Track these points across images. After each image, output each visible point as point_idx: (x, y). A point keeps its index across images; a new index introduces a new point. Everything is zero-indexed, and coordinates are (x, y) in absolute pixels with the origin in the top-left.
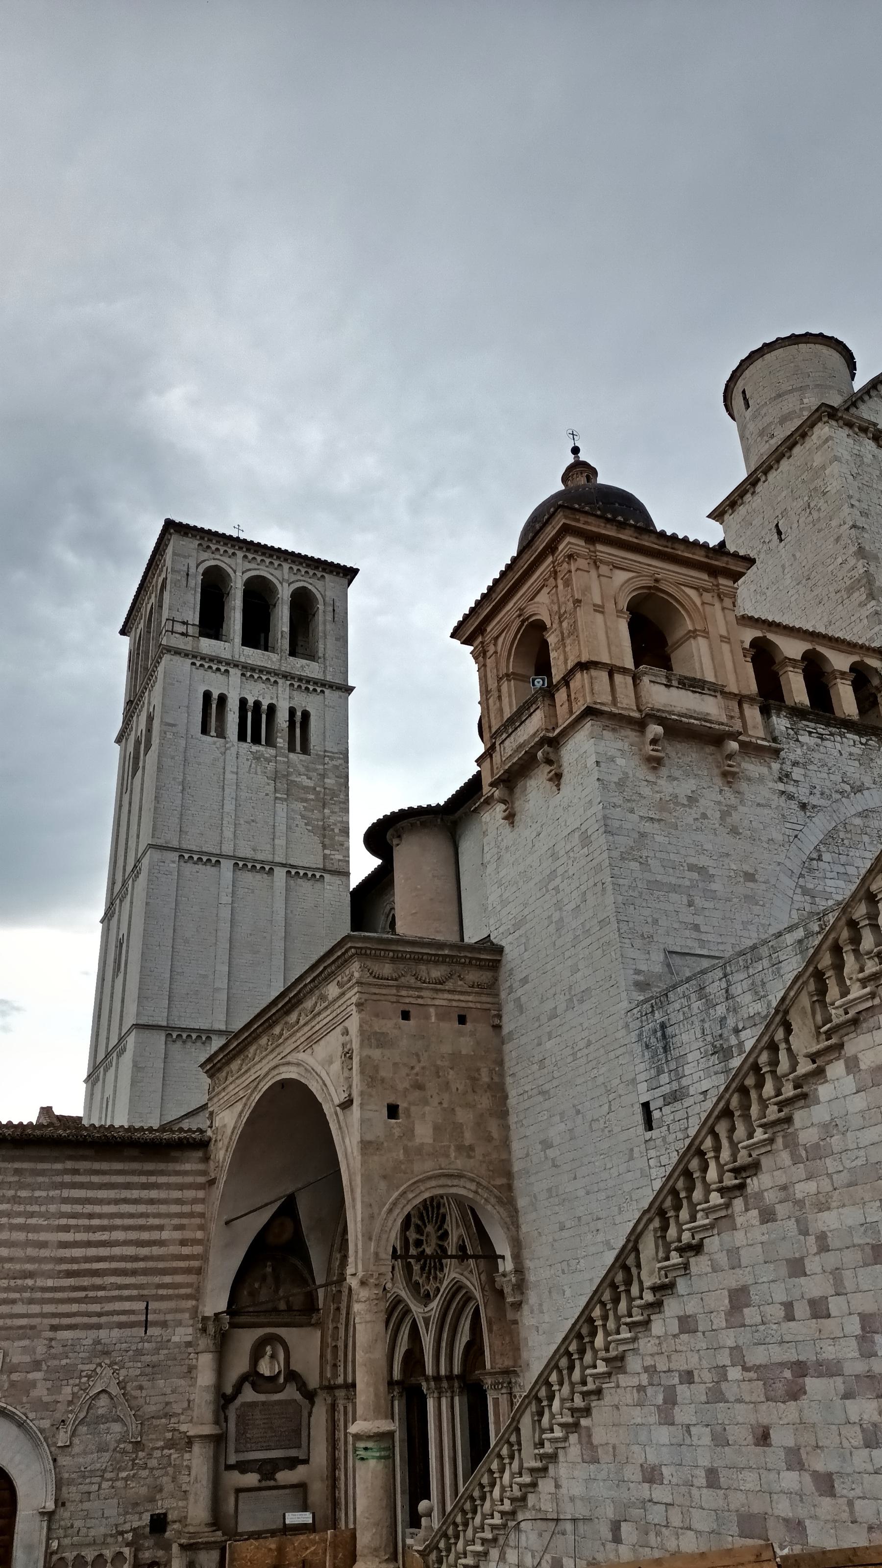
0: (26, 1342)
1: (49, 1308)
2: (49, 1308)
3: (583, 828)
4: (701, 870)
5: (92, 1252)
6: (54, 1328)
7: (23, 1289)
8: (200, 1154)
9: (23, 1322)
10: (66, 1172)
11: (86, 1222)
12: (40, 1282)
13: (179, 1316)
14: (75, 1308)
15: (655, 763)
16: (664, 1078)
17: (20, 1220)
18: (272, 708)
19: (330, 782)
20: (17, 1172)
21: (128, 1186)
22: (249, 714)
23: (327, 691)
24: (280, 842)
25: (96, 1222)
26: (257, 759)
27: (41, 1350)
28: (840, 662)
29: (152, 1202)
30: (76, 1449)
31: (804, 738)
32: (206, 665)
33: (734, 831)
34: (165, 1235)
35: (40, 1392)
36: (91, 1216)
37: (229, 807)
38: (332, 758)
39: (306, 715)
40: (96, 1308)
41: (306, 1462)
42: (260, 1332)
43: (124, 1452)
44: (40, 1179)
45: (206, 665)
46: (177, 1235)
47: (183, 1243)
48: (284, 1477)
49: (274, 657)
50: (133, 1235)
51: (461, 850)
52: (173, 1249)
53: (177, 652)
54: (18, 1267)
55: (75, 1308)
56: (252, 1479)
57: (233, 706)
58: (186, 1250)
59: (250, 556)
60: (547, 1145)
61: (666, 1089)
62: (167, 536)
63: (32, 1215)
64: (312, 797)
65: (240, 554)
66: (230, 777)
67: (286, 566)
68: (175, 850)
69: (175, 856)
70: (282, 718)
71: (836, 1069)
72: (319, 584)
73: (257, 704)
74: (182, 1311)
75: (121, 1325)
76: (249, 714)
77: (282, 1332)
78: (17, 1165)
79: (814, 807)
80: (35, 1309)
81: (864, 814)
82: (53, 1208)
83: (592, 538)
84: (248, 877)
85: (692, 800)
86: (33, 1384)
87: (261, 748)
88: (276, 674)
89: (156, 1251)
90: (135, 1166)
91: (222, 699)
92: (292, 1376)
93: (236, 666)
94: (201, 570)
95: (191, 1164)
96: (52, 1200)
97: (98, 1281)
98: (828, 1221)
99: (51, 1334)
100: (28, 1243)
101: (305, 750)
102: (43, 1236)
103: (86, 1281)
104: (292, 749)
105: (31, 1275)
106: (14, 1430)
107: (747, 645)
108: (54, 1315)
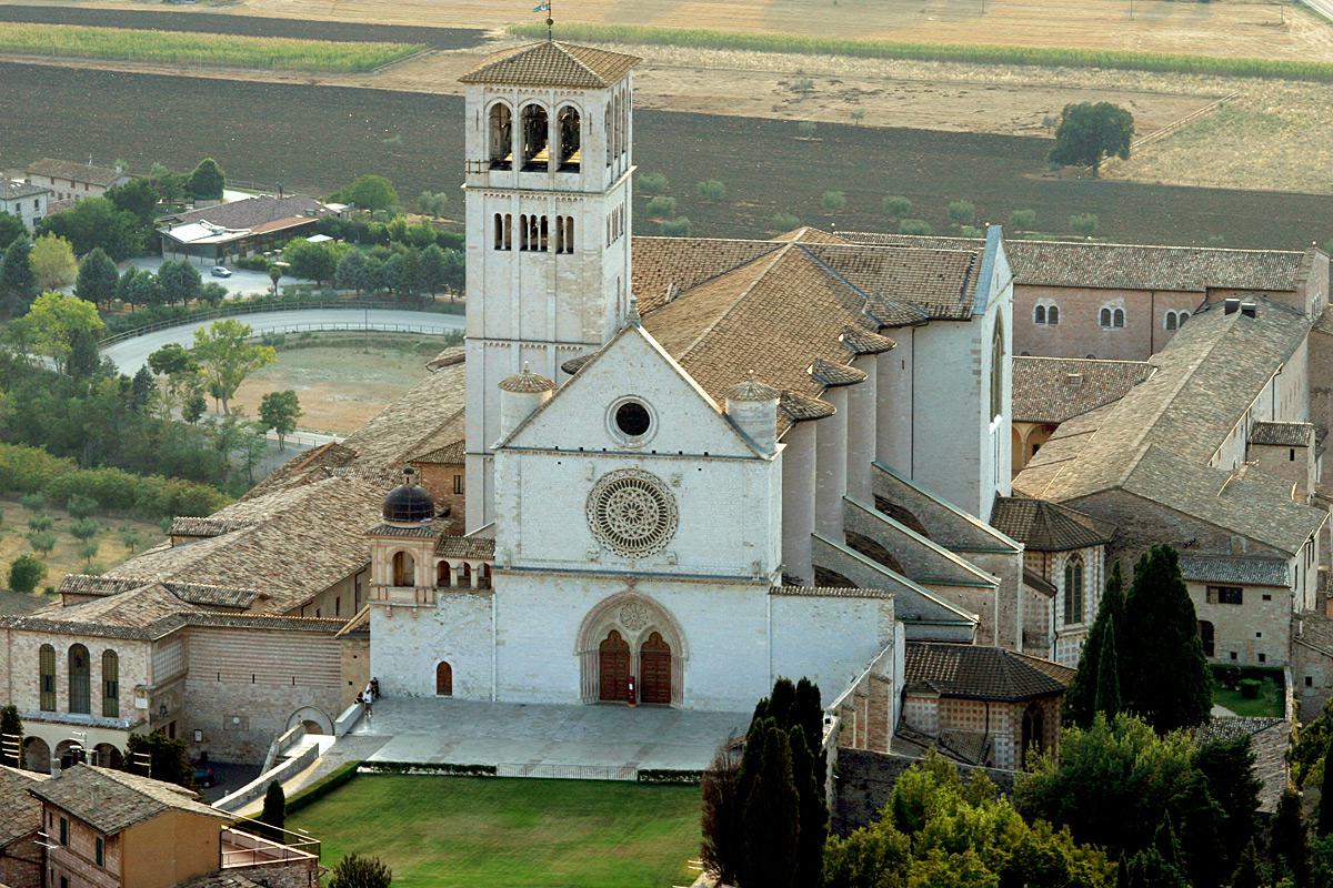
18: (544, 218)
23: (585, 199)
31: (449, 599)
33: (415, 634)
35: (326, 704)
37: (515, 304)
39: (570, 219)
57: (516, 223)
59: (523, 89)
65: (516, 89)
67: (552, 91)
70: (552, 226)
73: (533, 218)
79: (447, 624)
81: (468, 623)
85: (401, 626)
91: (508, 216)
94: (488, 110)
101: (570, 251)
104: (560, 251)
107: (436, 565)
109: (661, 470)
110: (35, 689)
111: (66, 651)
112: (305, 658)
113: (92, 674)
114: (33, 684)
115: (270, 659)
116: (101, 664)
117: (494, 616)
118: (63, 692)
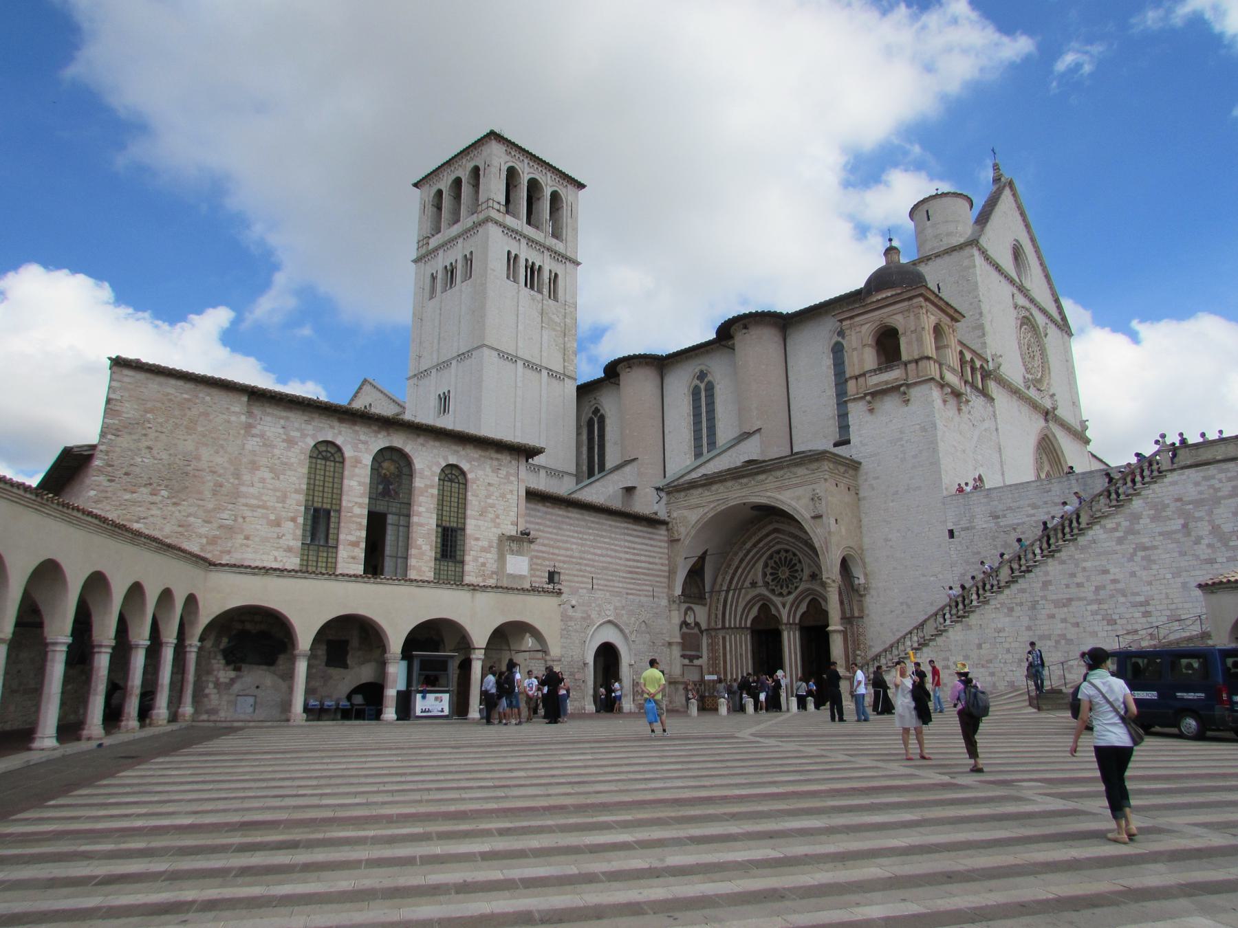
0: (618, 598)
1: (625, 585)
2: (625, 585)
3: (922, 425)
4: (955, 447)
5: (635, 564)
6: (627, 594)
7: (616, 576)
8: (664, 527)
9: (618, 590)
10: (625, 528)
11: (632, 551)
12: (621, 574)
13: (662, 595)
14: (632, 586)
15: (945, 401)
16: (962, 522)
17: (613, 547)
19: (568, 321)
20: (610, 526)
21: (644, 538)
22: (529, 270)
23: (568, 263)
24: (544, 354)
25: (636, 551)
26: (533, 300)
27: (624, 601)
28: (978, 364)
29: (651, 546)
30: (637, 643)
32: (510, 234)
34: (657, 560)
36: (634, 549)
38: (569, 307)
39: (556, 275)
40: (638, 588)
41: (701, 657)
42: (687, 605)
43: (650, 646)
44: (617, 530)
45: (510, 234)
46: (661, 561)
47: (662, 565)
48: (696, 662)
49: (542, 235)
50: (647, 559)
51: (665, 381)
52: (659, 567)
53: (496, 222)
54: (614, 567)
55: (632, 586)
56: (686, 662)
57: (522, 263)
58: (663, 568)
59: (531, 164)
60: (886, 540)
61: (964, 526)
62: (487, 139)
63: (616, 545)
64: (559, 329)
65: (526, 161)
66: (520, 308)
67: (549, 174)
68: (496, 350)
69: (496, 353)
71: (1096, 527)
72: (564, 190)
73: (533, 263)
74: (663, 593)
75: (646, 596)
76: (529, 270)
77: (693, 606)
78: (610, 523)
80: (621, 585)
81: (986, 430)
82: (622, 543)
83: (927, 299)
84: (529, 372)
86: (622, 615)
87: (536, 294)
88: (544, 247)
89: (655, 567)
90: (645, 529)
91: (516, 256)
92: (697, 624)
93: (525, 237)
95: (662, 531)
96: (621, 540)
97: (638, 576)
98: (1085, 564)
99: (625, 596)
100: (616, 557)
101: (556, 299)
102: (622, 555)
103: (635, 576)
104: (550, 297)
105: (617, 570)
106: (619, 633)
108: (628, 589)
109: (1040, 319)
110: (293, 533)
111: (367, 460)
112: (604, 552)
113: (416, 508)
114: (291, 524)
115: (567, 549)
116: (435, 492)
117: (999, 426)
118: (355, 544)
